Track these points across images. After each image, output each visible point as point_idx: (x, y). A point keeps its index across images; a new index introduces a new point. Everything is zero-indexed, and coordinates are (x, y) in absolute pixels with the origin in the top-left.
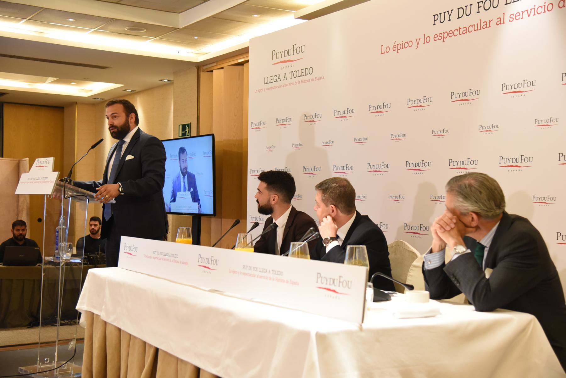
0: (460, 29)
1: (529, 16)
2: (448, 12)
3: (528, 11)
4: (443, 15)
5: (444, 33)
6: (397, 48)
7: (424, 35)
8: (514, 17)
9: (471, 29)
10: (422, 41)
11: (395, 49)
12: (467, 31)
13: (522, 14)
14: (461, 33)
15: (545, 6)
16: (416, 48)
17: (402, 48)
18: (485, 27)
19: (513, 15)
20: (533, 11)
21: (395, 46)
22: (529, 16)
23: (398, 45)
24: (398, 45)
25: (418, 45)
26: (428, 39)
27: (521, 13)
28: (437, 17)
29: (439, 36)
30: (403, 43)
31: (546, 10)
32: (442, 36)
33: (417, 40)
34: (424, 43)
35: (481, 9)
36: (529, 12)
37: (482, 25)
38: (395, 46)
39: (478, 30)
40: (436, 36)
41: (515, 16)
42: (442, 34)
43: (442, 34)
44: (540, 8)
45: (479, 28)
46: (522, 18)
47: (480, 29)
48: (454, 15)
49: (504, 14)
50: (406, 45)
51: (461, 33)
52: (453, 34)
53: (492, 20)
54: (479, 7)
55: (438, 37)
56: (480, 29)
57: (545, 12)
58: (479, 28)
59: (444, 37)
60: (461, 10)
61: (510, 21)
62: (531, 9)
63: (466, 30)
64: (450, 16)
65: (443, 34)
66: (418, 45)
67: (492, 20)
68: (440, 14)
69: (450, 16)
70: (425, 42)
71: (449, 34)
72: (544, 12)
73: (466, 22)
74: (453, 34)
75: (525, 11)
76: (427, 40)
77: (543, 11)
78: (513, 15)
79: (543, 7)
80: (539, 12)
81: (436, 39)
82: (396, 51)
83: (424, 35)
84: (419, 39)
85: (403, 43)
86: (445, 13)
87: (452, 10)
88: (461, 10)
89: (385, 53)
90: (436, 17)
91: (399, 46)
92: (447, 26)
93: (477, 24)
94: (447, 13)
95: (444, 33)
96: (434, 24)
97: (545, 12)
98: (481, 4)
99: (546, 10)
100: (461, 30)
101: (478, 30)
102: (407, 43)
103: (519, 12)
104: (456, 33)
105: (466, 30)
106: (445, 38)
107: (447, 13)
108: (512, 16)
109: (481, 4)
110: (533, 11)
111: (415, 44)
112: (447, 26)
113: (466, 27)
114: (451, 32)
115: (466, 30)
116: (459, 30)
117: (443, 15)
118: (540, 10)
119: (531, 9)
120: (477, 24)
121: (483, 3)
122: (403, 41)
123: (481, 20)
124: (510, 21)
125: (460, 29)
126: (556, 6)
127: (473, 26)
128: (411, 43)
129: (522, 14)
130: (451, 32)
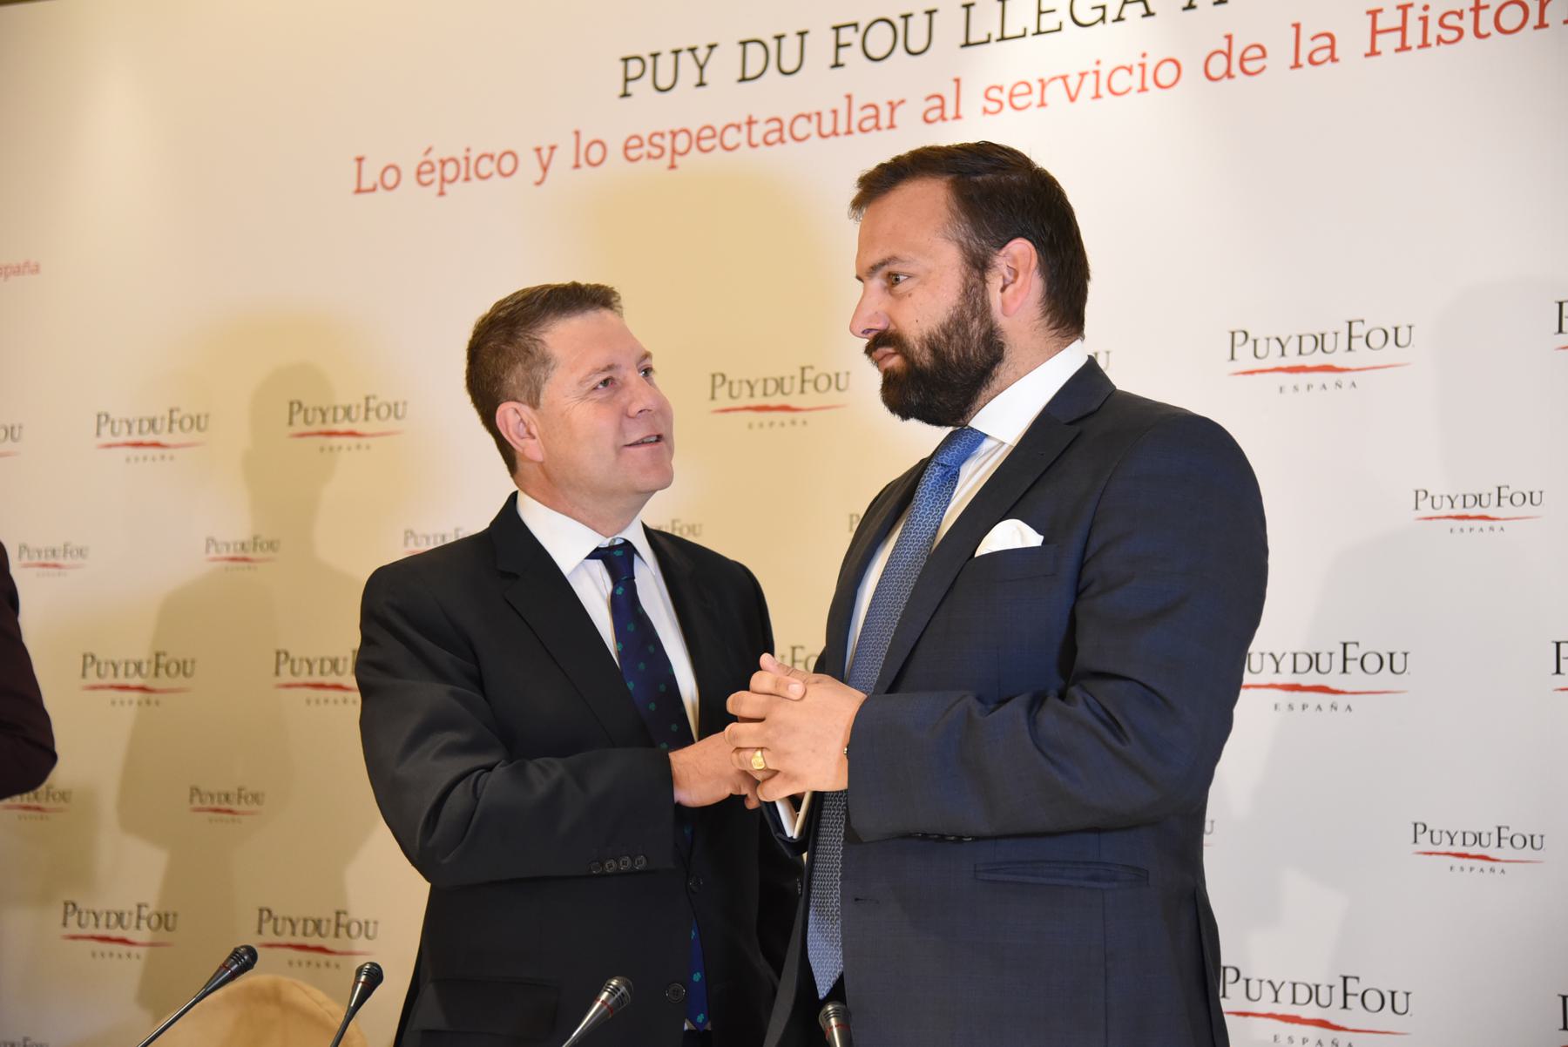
0: (750, 122)
1: (1072, 99)
2: (692, 50)
3: (1069, 80)
4: (666, 62)
5: (674, 134)
6: (437, 176)
7: (577, 133)
8: (1004, 98)
9: (802, 128)
10: (564, 157)
11: (425, 178)
12: (787, 136)
13: (1043, 87)
14: (757, 138)
15: (1143, 66)
16: (538, 184)
17: (463, 175)
18: (868, 124)
19: (1001, 89)
20: (1090, 80)
21: (426, 168)
22: (1072, 99)
23: (443, 163)
24: (443, 163)
25: (545, 169)
26: (596, 149)
27: (1037, 87)
29: (651, 144)
30: (467, 159)
31: (1149, 83)
32: (667, 143)
33: (538, 150)
34: (577, 166)
35: (851, 56)
36: (1073, 82)
37: (857, 116)
38: (426, 168)
39: (835, 133)
40: (635, 142)
41: (1011, 96)
42: (662, 135)
43: (662, 135)
44: (1124, 73)
45: (842, 128)
46: (1043, 104)
47: (849, 132)
48: (724, 66)
49: (957, 81)
50: (486, 167)
51: (757, 138)
52: (716, 141)
53: (902, 102)
54: (838, 46)
55: (647, 148)
57: (1143, 89)
58: (842, 128)
59: (674, 151)
60: (755, 51)
61: (985, 111)
62: (1083, 75)
63: (781, 130)
64: (701, 68)
65: (668, 137)
66: (545, 169)
67: (902, 102)
68: (655, 56)
69: (701, 68)
70: (582, 161)
71: (699, 139)
72: (1139, 91)
74: (716, 141)
75: (1053, 79)
77: (1138, 86)
78: (1001, 89)
79: (1137, 71)
80: (1116, 88)
81: (633, 154)
82: (436, 187)
83: (577, 133)
84: (553, 148)
85: (467, 159)
87: (712, 47)
88: (755, 51)
89: (374, 189)
90: (635, 68)
91: (450, 170)
93: (835, 112)
94: (686, 58)
95: (674, 134)
97: (1143, 89)
98: (847, 35)
99: (1149, 83)
100: (758, 132)
101: (835, 133)
102: (492, 157)
103: (1029, 80)
104: (731, 137)
105: (781, 131)
106: (681, 154)
107: (686, 58)
108: (994, 94)
109: (847, 35)
110: (1090, 80)
111: (530, 166)
113: (778, 120)
114: (708, 133)
115: (781, 131)
116: (745, 128)
117: (666, 62)
118: (1121, 81)
119: (1083, 75)
120: (835, 112)
121: (857, 30)
122: (468, 150)
123: (849, 97)
124: (985, 111)
125: (750, 122)
126: (1193, 70)
127: (815, 119)
128: (507, 164)
129: (1043, 87)
130: (708, 133)
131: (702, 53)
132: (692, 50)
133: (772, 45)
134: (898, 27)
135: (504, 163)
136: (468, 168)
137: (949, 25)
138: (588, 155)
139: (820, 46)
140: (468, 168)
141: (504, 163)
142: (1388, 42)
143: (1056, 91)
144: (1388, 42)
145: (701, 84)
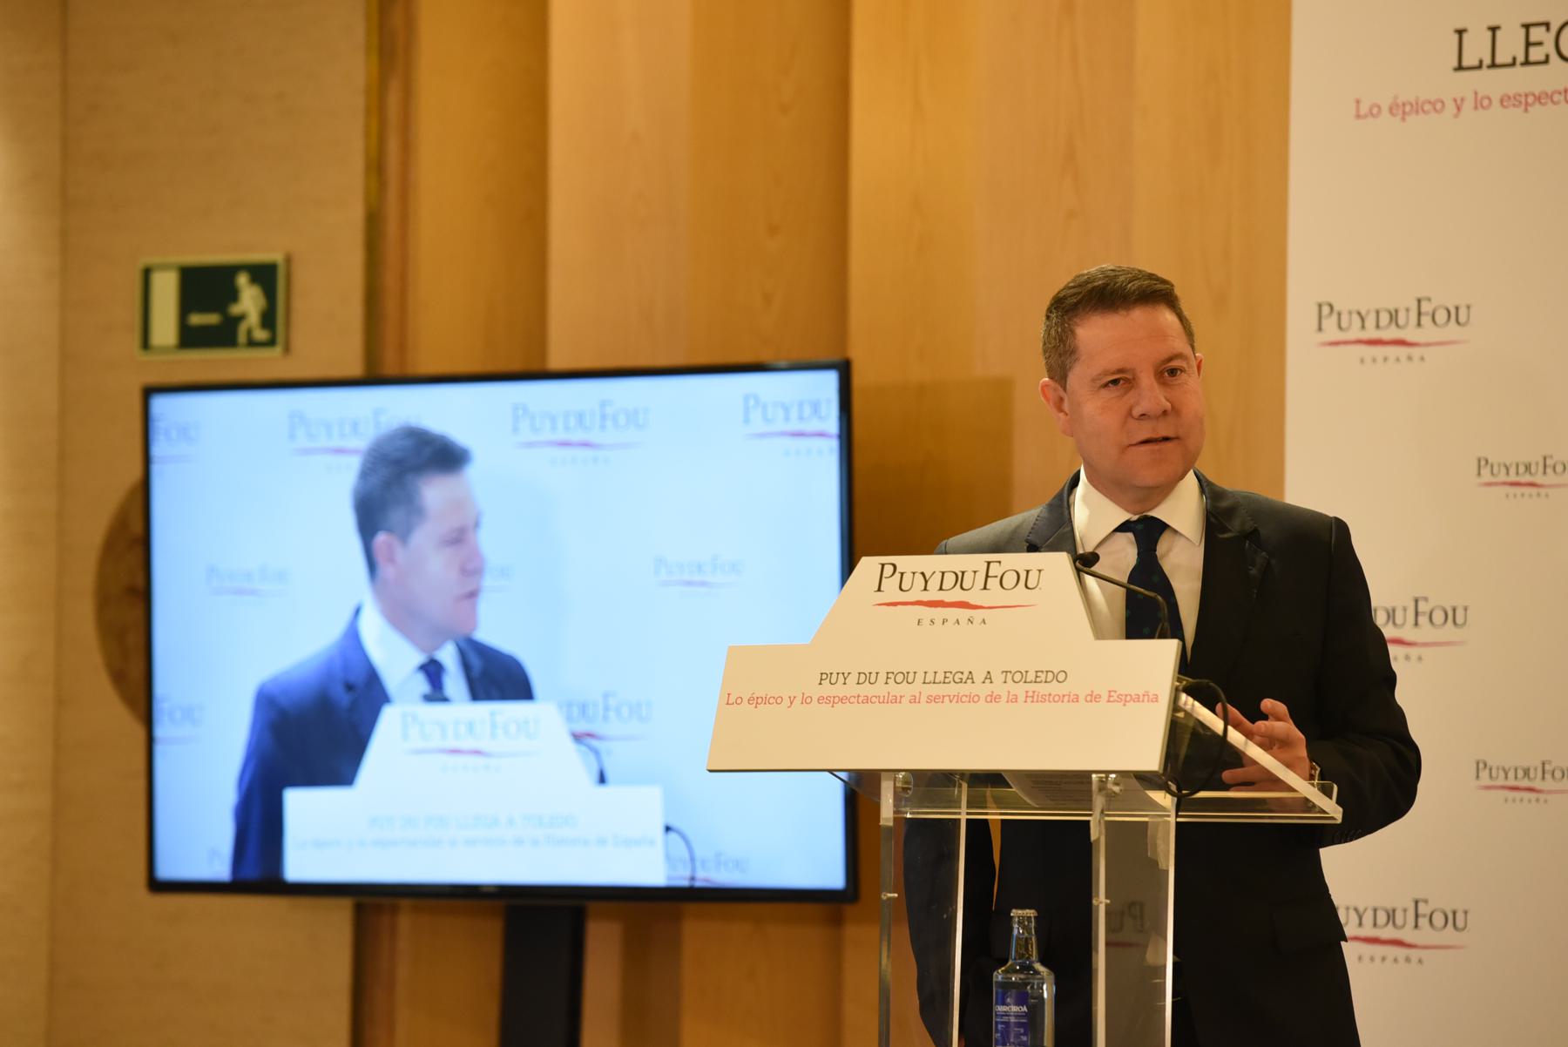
0: (859, 696)
2: (843, 674)
9: (874, 699)
10: (799, 699)
20: (956, 698)
28: (823, 677)
45: (886, 701)
48: (852, 679)
56: (888, 702)
58: (886, 701)
60: (862, 676)
68: (831, 674)
69: (845, 679)
73: (866, 690)
76: (806, 700)
86: (838, 674)
87: (849, 673)
88: (862, 676)
90: (824, 676)
91: (760, 700)
92: (839, 690)
94: (841, 675)
96: (820, 684)
104: (852, 700)
105: (867, 700)
107: (841, 675)
111: (786, 702)
112: (839, 690)
115: (867, 700)
118: (964, 699)
131: (846, 675)
132: (843, 674)
133: (868, 675)
134: (905, 675)
135: (778, 700)
136: (766, 700)
137: (920, 677)
138: (806, 700)
139: (882, 677)
140: (766, 700)
141: (778, 700)
142: (1029, 700)
143: (947, 699)
144: (1029, 700)
145: (845, 684)
